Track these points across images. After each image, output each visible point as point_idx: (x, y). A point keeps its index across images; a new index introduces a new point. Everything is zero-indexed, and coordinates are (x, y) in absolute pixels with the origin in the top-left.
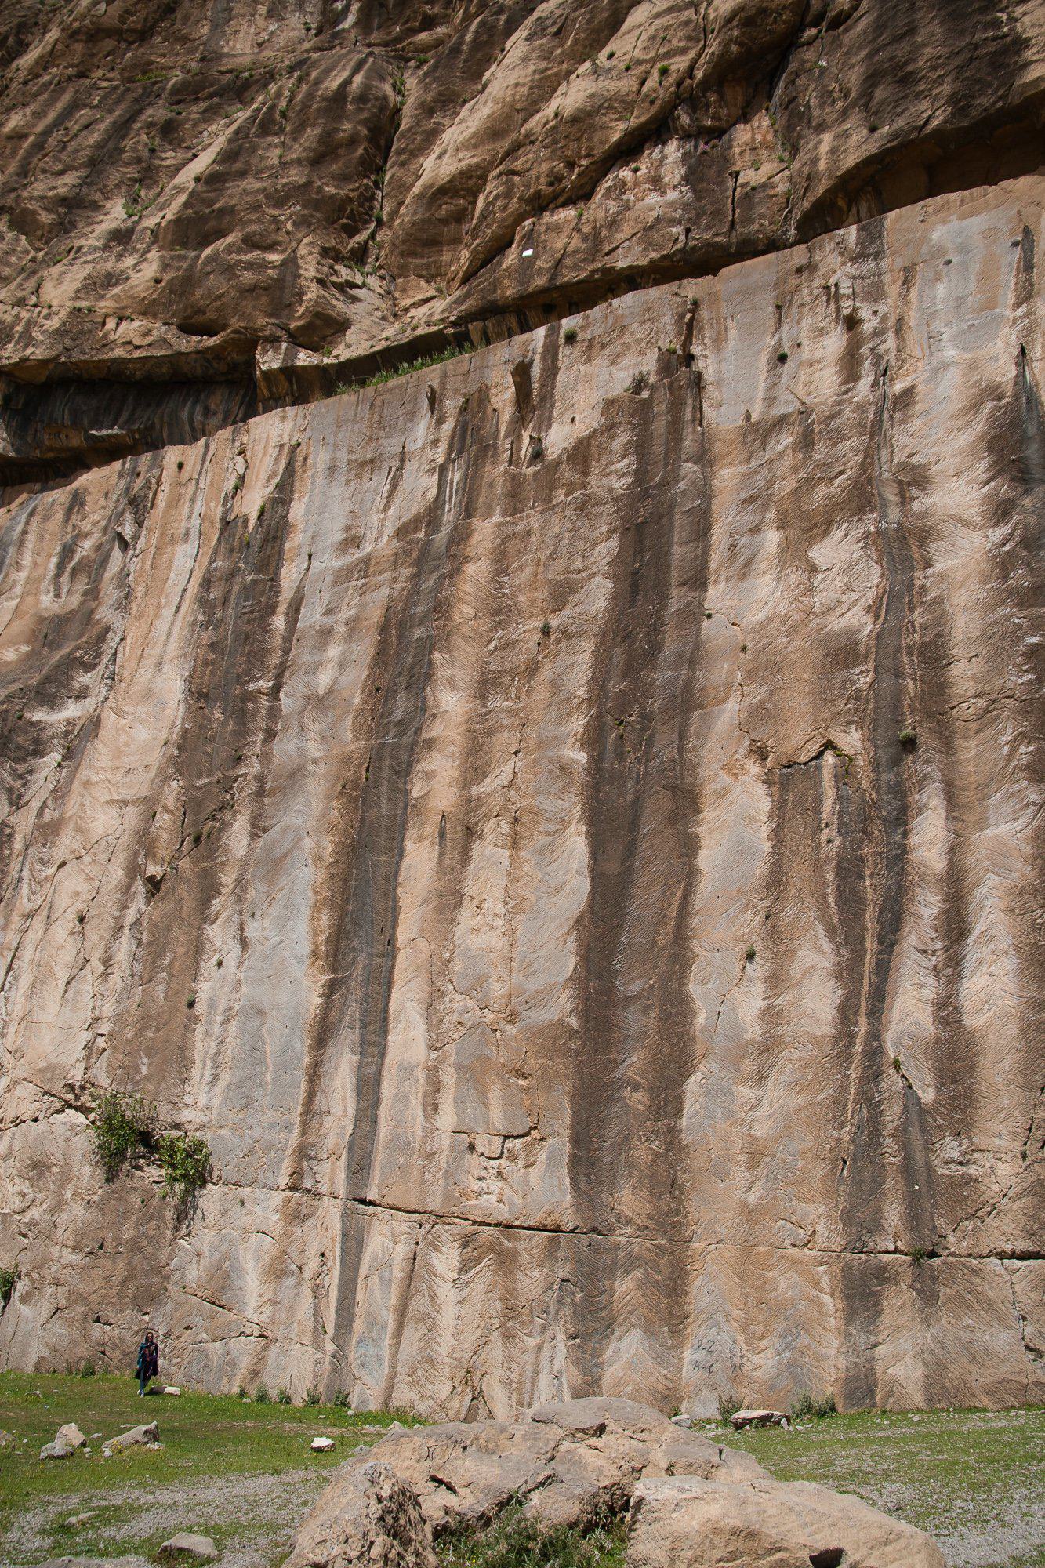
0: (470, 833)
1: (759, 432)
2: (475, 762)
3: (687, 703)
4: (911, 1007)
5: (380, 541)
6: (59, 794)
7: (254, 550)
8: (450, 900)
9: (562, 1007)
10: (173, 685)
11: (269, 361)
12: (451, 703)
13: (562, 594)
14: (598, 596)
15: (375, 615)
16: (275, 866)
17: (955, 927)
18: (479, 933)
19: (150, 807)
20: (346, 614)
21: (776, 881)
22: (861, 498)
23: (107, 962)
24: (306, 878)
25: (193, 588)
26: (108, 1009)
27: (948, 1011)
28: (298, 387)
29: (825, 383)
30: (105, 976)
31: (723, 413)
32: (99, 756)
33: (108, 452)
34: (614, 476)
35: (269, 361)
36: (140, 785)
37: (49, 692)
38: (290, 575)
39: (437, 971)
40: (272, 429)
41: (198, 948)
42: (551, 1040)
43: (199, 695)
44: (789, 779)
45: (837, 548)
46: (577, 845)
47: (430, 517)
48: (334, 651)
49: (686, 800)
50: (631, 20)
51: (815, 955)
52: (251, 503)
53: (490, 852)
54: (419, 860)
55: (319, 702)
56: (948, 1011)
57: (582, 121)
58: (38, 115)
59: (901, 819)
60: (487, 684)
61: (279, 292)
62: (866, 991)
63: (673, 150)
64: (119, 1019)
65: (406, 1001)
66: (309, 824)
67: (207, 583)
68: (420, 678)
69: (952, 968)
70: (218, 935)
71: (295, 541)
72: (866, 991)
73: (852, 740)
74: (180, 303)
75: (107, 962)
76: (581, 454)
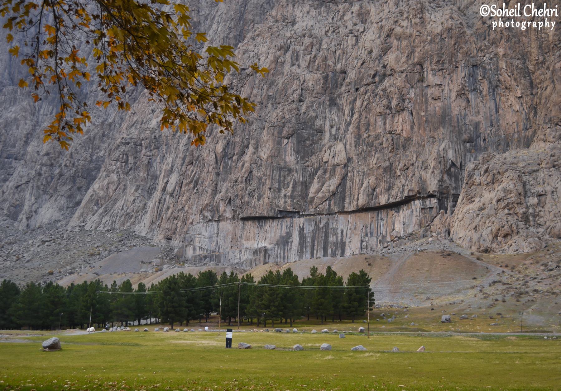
1: (332, 229)
2: (318, 247)
3: (328, 245)
5: (311, 231)
7: (302, 230)
8: (317, 254)
10: (298, 239)
11: (301, 213)
12: (316, 243)
13: (322, 237)
14: (323, 238)
16: (307, 252)
22: (336, 234)
24: (309, 252)
28: (303, 216)
29: (335, 226)
31: (330, 227)
32: (293, 244)
34: (324, 230)
35: (301, 213)
36: (297, 245)
37: (289, 238)
38: (305, 232)
40: (302, 219)
44: (332, 249)
45: (334, 237)
47: (314, 230)
49: (327, 250)
50: (325, 185)
52: (301, 225)
54: (315, 252)
55: (308, 242)
57: (322, 198)
58: (270, 171)
60: (318, 242)
61: (301, 206)
63: (328, 202)
66: (309, 249)
68: (314, 241)
74: (292, 205)
76: (322, 228)
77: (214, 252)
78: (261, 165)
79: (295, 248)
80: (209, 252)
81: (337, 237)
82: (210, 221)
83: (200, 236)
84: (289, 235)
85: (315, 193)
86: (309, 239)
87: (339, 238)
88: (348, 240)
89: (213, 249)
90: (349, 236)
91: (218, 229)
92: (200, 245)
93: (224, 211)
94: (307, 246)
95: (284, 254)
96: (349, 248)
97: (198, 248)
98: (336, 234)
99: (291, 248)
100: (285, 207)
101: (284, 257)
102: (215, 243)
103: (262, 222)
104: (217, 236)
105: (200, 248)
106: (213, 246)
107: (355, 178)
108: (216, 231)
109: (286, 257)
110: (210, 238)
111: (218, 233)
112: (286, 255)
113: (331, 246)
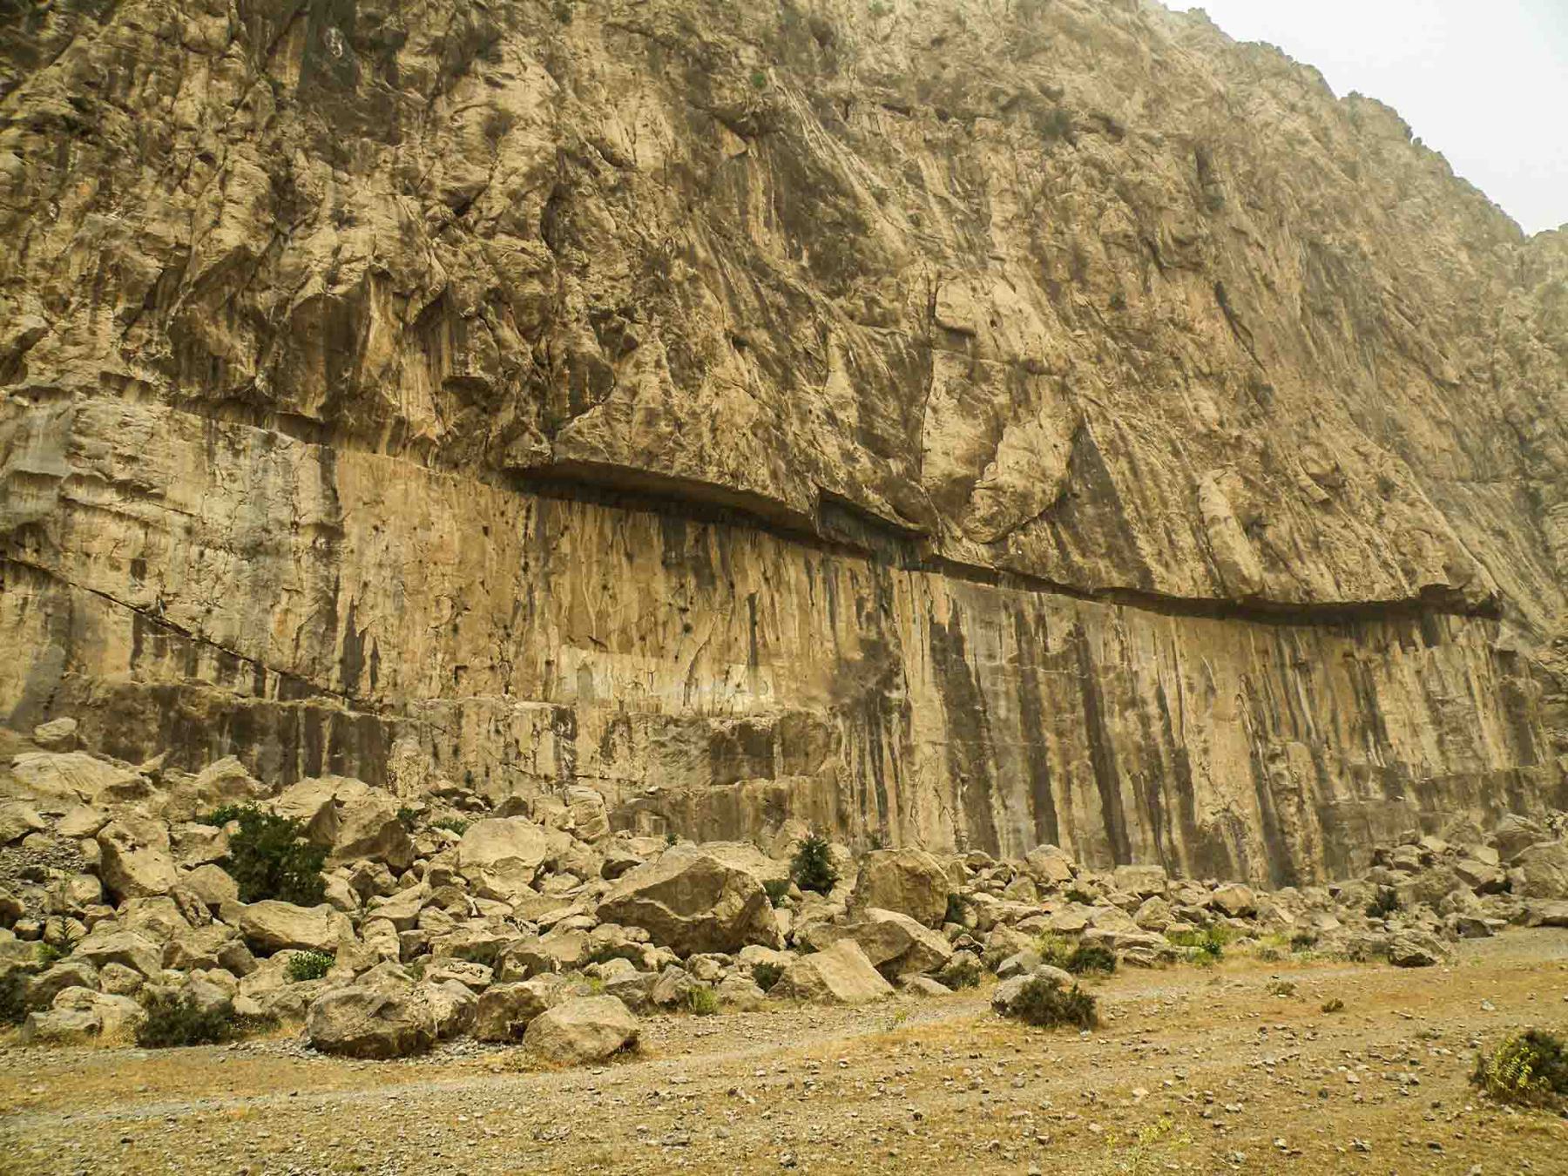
0: (1069, 782)
4: (1164, 839)
6: (906, 734)
8: (1068, 801)
9: (1103, 834)
13: (1073, 708)
15: (1014, 694)
17: (1169, 822)
18: (1078, 812)
19: (951, 750)
20: (1001, 687)
21: (1137, 807)
23: (954, 808)
24: (1021, 788)
25: (927, 651)
26: (962, 825)
27: (1171, 841)
30: (956, 814)
33: (856, 551)
36: (940, 736)
39: (1070, 822)
41: (990, 808)
42: (1102, 843)
43: (947, 701)
44: (1134, 779)
45: (1130, 714)
46: (1095, 789)
48: (1002, 703)
51: (1148, 827)
52: (944, 618)
53: (1075, 786)
54: (1055, 787)
56: (1171, 841)
59: (1156, 795)
62: (1157, 838)
64: (969, 831)
65: (1061, 828)
67: (933, 649)
69: (1169, 832)
70: (995, 801)
71: (967, 646)
72: (1157, 838)
73: (1146, 772)
75: (954, 808)
77: (293, 682)
78: (625, 184)
79: (928, 750)
80: (245, 681)
81: (1145, 720)
82: (248, 405)
83: (146, 509)
84: (880, 657)
85: (970, 462)
86: (1004, 710)
87: (1157, 727)
88: (1193, 745)
89: (282, 655)
90: (1190, 718)
91: (332, 496)
92: (148, 593)
93: (386, 370)
94: (1007, 751)
95: (880, 783)
96: (1204, 781)
97: (117, 628)
98: (1134, 702)
99: (908, 750)
100: (852, 483)
101: (883, 797)
102: (306, 607)
103: (701, 540)
104: (328, 556)
105: (148, 620)
106: (282, 632)
107: (1139, 454)
108: (311, 507)
109: (892, 803)
110: (253, 551)
111: (331, 531)
112: (889, 784)
113: (1126, 761)
